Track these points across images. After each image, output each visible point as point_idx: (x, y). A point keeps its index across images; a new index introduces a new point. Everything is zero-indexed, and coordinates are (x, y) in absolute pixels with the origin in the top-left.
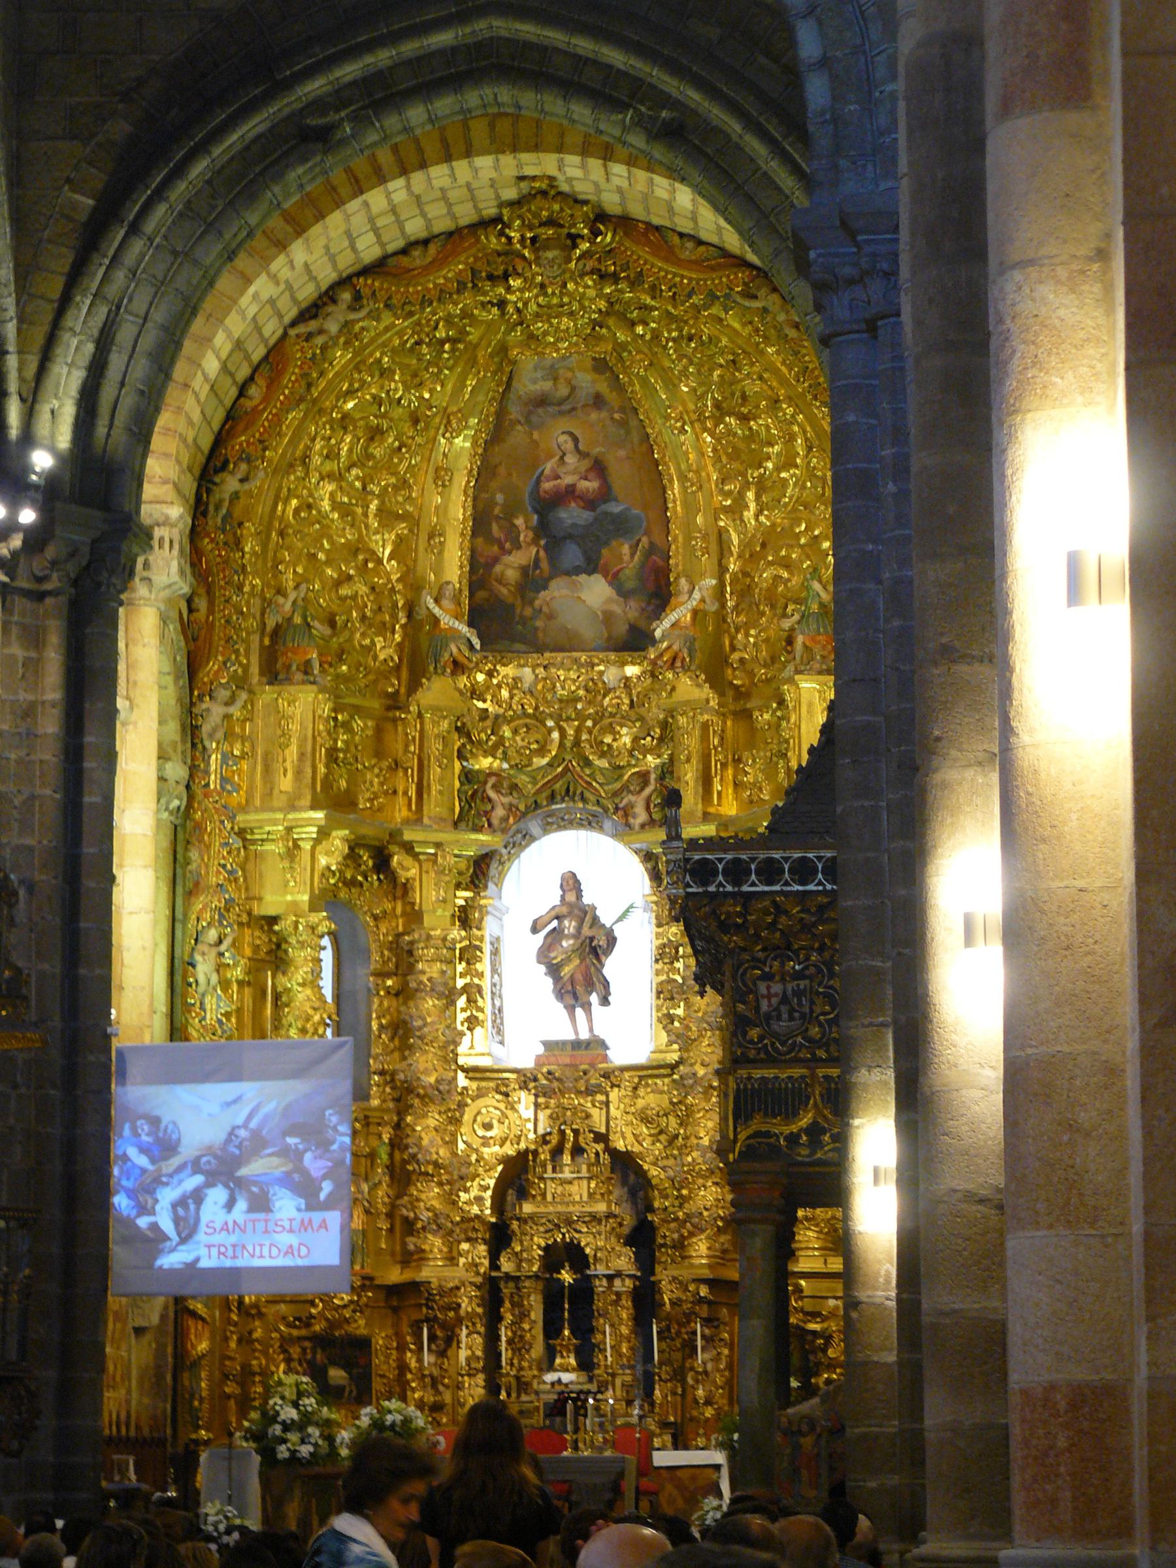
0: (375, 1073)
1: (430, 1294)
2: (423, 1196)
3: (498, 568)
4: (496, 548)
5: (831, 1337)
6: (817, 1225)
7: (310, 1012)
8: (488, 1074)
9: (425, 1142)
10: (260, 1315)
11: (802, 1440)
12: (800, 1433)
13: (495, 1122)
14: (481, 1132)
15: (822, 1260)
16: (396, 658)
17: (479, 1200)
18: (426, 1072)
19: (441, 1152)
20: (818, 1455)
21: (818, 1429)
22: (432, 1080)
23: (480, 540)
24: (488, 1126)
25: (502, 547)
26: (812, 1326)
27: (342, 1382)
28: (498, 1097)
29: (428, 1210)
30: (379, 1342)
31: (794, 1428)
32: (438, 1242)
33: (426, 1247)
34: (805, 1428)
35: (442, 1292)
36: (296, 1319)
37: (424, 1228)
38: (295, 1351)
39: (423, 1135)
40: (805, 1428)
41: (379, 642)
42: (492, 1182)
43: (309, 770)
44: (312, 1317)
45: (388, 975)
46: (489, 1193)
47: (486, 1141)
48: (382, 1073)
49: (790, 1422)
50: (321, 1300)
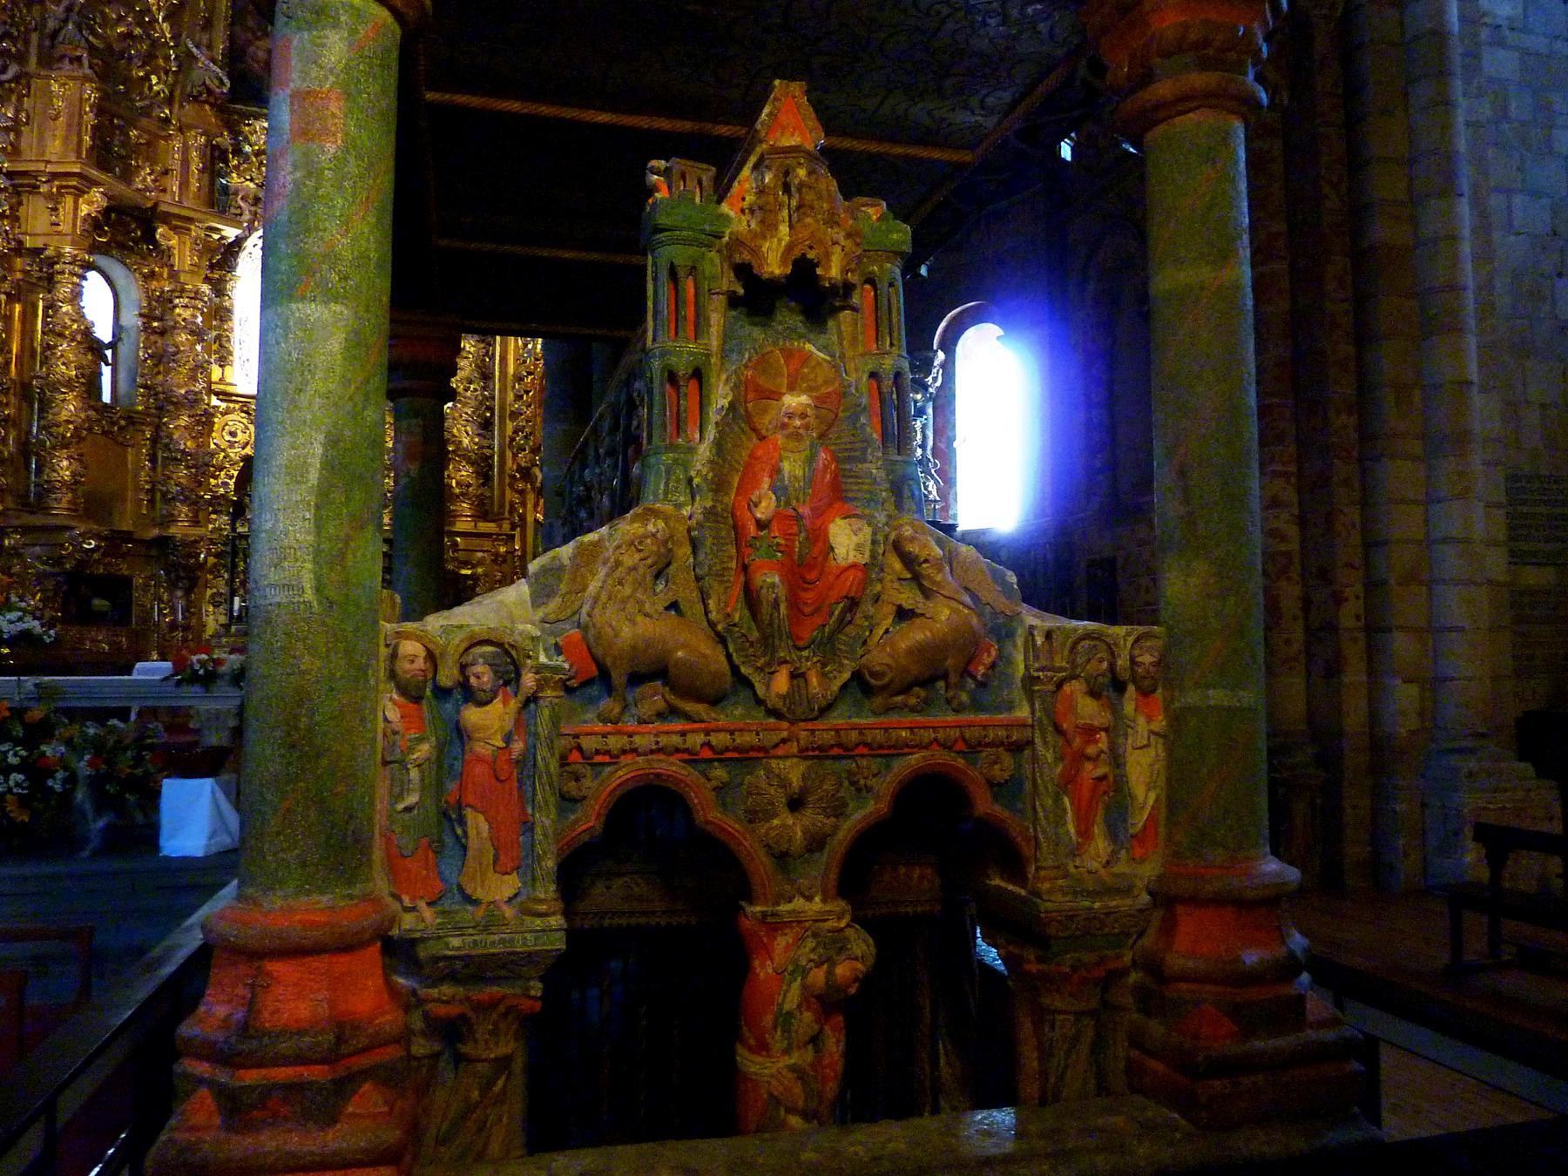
0: (141, 387)
1: (175, 545)
2: (174, 476)
3: (252, 49)
4: (250, 35)
5: (479, 579)
6: (469, 499)
7: (69, 323)
8: (234, 398)
9: (175, 437)
10: (19, 555)
11: (472, 715)
12: (469, 694)
13: (239, 432)
14: (228, 438)
15: (473, 524)
16: (166, 91)
17: (225, 484)
18: (180, 387)
19: (189, 444)
20: (526, 762)
21: (529, 680)
22: (183, 391)
23: (238, 29)
24: (233, 434)
25: (254, 33)
26: (464, 572)
27: (105, 609)
28: (243, 415)
29: (176, 485)
30: (138, 581)
31: (448, 676)
32: (185, 509)
33: (176, 513)
34: (483, 675)
35: (184, 544)
36: (49, 559)
37: (173, 498)
38: (50, 584)
39: (174, 431)
40: (483, 675)
41: (154, 79)
42: (236, 473)
43: (75, 138)
44: (63, 557)
45: (156, 319)
46: (234, 480)
47: (232, 445)
48: (145, 387)
49: (431, 656)
50: (71, 544)
